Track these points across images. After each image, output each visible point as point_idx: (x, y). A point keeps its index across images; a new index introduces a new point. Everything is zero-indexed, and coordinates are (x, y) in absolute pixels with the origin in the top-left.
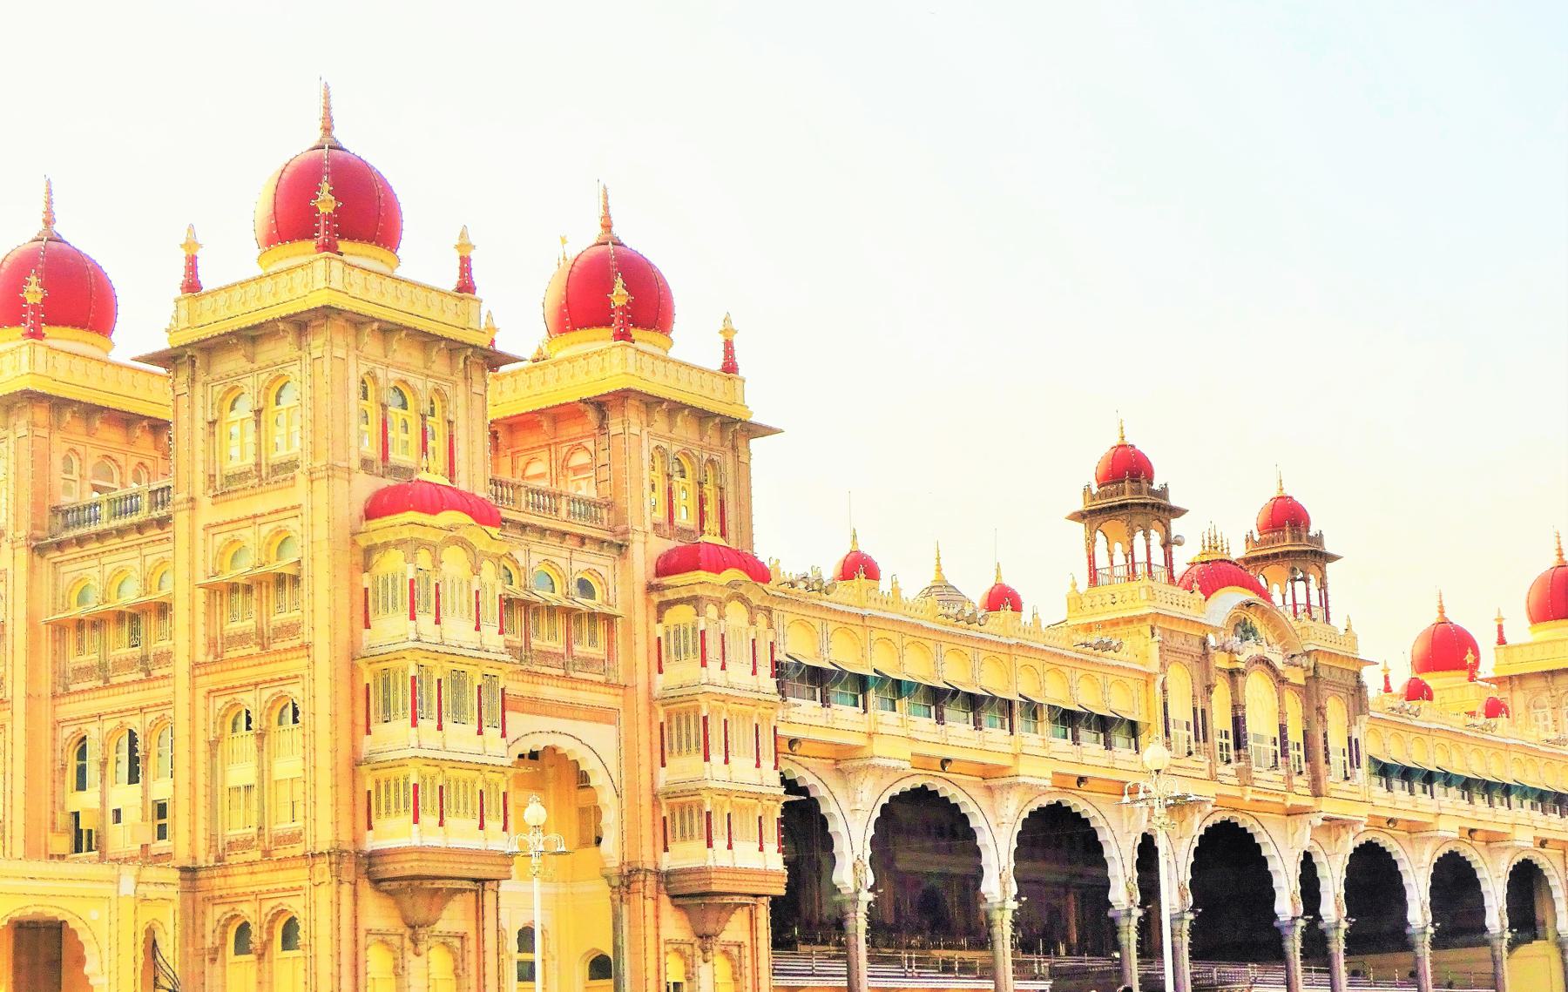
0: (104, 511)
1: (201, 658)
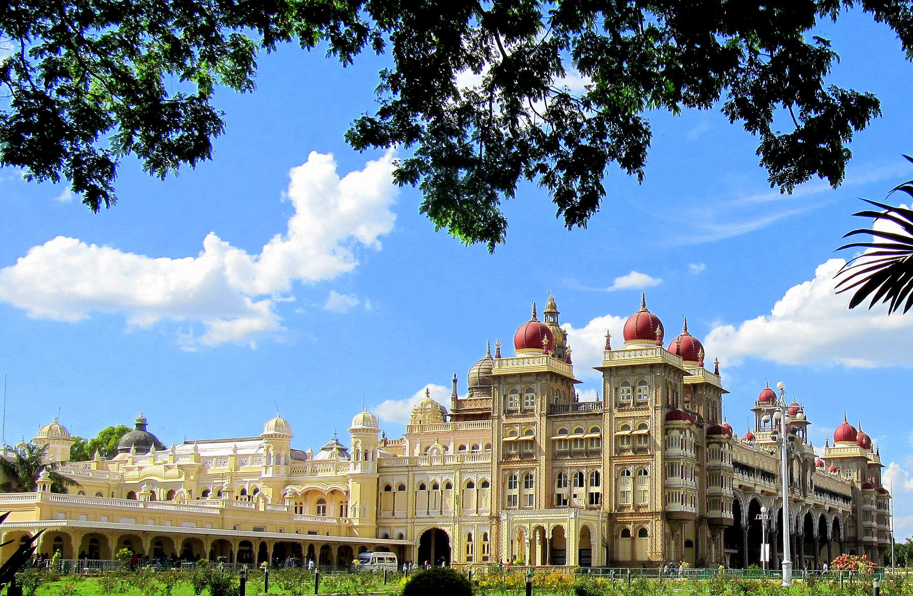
0: (570, 409)
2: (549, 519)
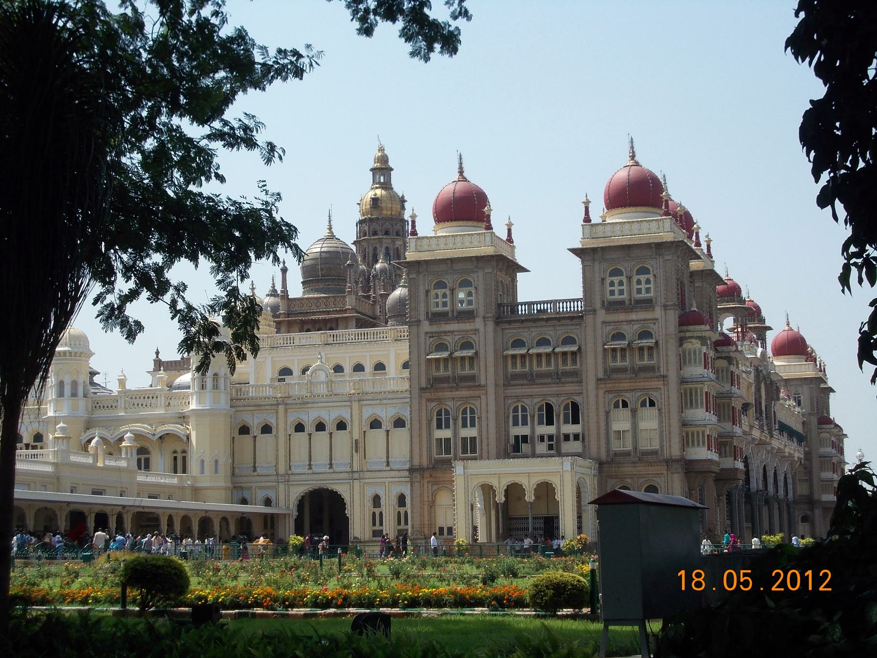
1: (601, 376)
2: (527, 472)
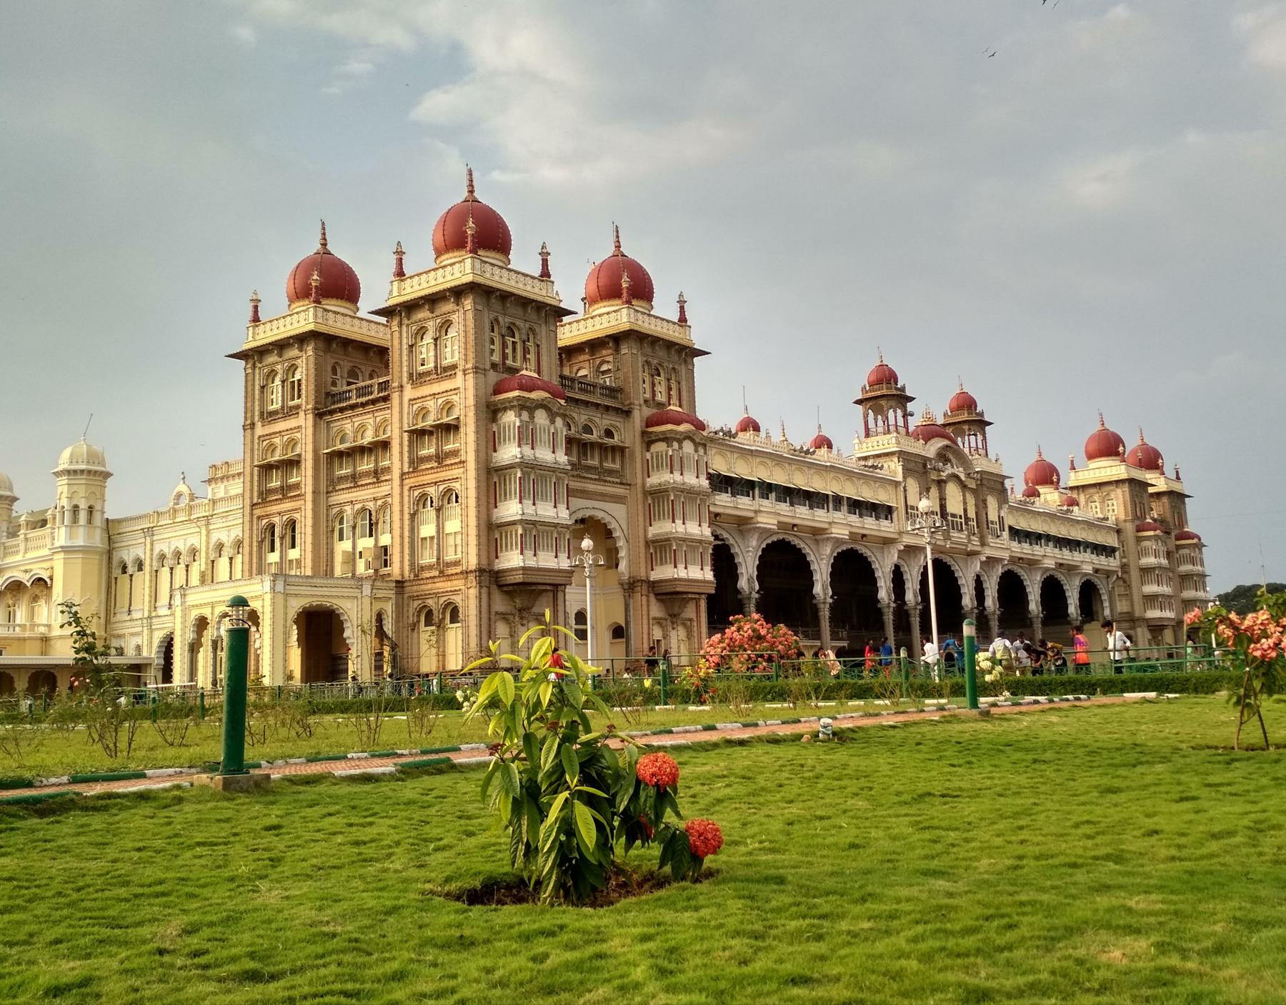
1: (406, 470)
